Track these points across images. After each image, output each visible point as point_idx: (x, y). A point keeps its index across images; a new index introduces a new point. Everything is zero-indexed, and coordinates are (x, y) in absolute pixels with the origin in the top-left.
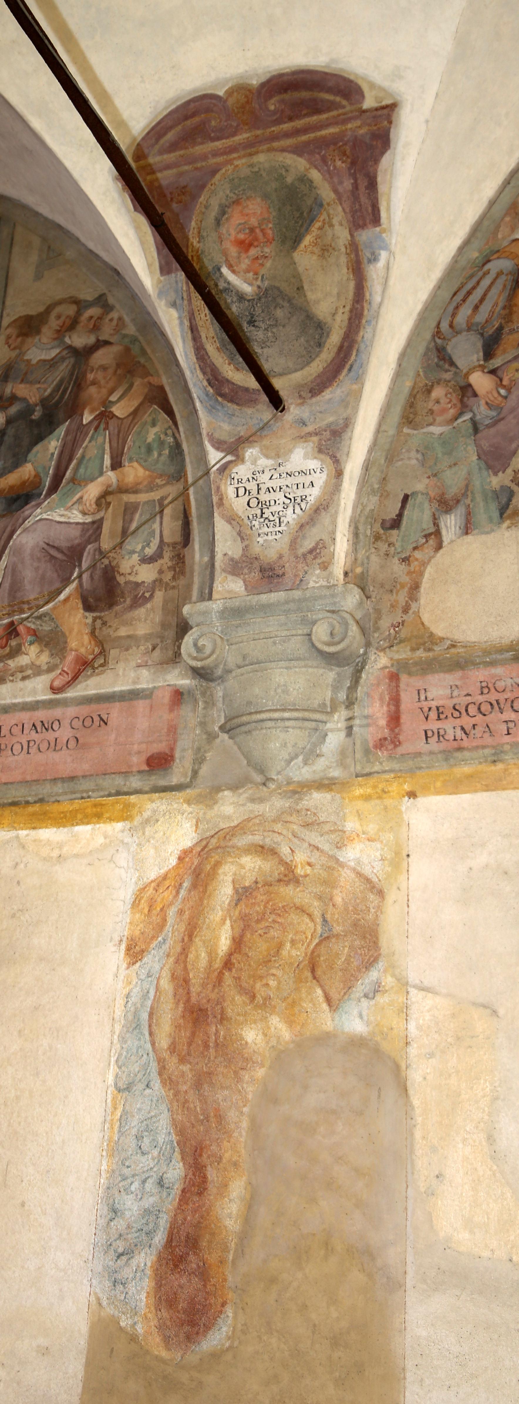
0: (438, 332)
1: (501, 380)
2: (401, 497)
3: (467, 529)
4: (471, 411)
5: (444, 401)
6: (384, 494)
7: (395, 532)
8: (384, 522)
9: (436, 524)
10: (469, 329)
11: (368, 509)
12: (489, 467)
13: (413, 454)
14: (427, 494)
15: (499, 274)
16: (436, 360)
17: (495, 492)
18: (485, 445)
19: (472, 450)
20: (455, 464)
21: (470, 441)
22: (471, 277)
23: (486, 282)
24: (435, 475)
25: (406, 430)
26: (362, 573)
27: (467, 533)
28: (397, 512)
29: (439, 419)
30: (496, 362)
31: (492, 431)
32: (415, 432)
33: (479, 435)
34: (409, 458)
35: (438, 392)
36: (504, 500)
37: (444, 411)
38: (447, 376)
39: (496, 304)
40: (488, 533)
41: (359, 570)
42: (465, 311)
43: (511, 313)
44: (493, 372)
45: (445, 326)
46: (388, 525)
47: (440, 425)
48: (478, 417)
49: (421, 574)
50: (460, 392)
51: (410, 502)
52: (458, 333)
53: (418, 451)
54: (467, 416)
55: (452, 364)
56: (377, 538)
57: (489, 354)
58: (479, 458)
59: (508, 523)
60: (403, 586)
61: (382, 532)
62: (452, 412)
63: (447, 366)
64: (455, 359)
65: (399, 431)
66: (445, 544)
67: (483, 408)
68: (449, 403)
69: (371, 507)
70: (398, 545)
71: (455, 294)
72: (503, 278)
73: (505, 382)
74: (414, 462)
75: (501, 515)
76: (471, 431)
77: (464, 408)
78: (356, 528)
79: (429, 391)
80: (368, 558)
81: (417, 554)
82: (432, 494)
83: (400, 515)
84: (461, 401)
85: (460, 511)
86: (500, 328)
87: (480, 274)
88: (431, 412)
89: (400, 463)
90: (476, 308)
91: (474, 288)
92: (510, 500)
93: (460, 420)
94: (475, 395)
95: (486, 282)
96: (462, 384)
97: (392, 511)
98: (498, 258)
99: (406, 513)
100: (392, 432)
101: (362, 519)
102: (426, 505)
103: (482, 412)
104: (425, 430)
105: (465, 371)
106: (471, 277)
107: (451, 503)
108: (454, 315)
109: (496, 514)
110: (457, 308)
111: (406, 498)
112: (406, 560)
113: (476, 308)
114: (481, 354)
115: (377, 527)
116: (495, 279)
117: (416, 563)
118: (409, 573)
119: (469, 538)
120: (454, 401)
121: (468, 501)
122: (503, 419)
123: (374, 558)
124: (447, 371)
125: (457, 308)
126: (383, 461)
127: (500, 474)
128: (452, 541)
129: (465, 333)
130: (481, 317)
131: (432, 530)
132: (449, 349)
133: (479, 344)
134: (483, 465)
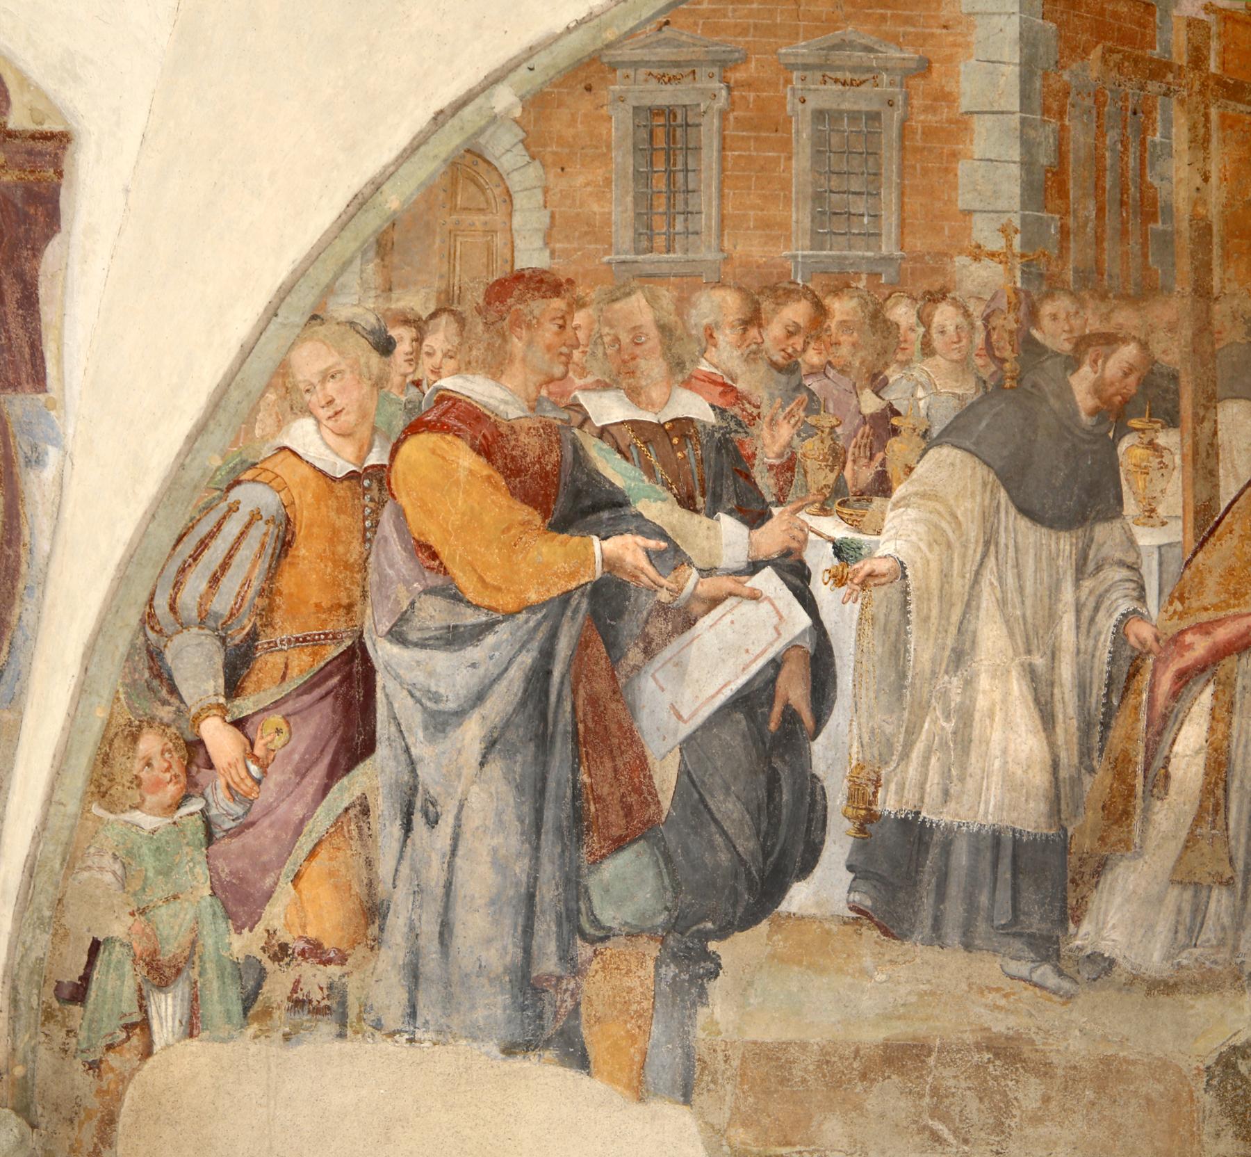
0: (151, 616)
1: (252, 744)
2: (88, 944)
3: (192, 1027)
4: (202, 795)
5: (158, 763)
6: (61, 934)
7: (76, 1009)
8: (59, 986)
9: (143, 1008)
10: (202, 624)
11: (33, 955)
12: (229, 915)
13: (107, 860)
14: (130, 947)
15: (255, 516)
16: (147, 675)
17: (236, 964)
18: (224, 868)
19: (202, 871)
20: (175, 897)
21: (200, 855)
22: (208, 508)
23: (232, 528)
24: (143, 912)
25: (96, 810)
26: (25, 1077)
27: (191, 1035)
28: (81, 972)
29: (151, 799)
30: (245, 706)
31: (236, 843)
32: (112, 817)
33: (214, 847)
34: (101, 869)
35: (150, 743)
36: (250, 984)
37: (158, 785)
38: (165, 713)
39: (247, 582)
40: (223, 1041)
41: (19, 1071)
42: (196, 583)
43: (271, 609)
44: (239, 724)
45: (162, 603)
46: (66, 993)
47: (151, 812)
48: (213, 812)
49: (119, 1098)
50: (184, 752)
51: (102, 956)
52: (184, 626)
53: (115, 857)
54: (195, 805)
55: (173, 690)
56: (49, 1016)
57: (233, 688)
58: (214, 894)
59: (253, 1028)
60: (89, 1117)
61: (56, 1005)
62: (172, 790)
63: (164, 692)
64: (178, 681)
65: (85, 811)
66: (156, 1048)
67: (222, 794)
68: (168, 769)
69: (37, 952)
70: (82, 1034)
71: (180, 540)
72: (259, 530)
73: (259, 751)
74: (108, 877)
75: (246, 1010)
76: (201, 836)
77: (191, 789)
78: (14, 988)
79: (135, 738)
80: (34, 1050)
81: (112, 1059)
82: (138, 949)
83: (86, 978)
84: (187, 771)
85: (181, 989)
86: (253, 636)
87: (223, 506)
88: (137, 781)
89: (86, 874)
90: (215, 580)
91: (212, 535)
92: (259, 986)
93: (184, 811)
94: (210, 766)
95: (232, 528)
96: (190, 737)
97: (73, 973)
98: (254, 480)
99: (95, 975)
100: (73, 807)
101: (24, 974)
102: (128, 966)
103: (223, 806)
104: (127, 817)
105: (194, 711)
106: (208, 508)
107: (167, 972)
108: (177, 585)
109: (237, 1008)
110: (183, 571)
111: (95, 947)
112: (94, 1066)
113: (215, 580)
114: (221, 681)
115: (49, 993)
116: (248, 526)
117: (111, 1075)
118: (100, 1092)
119: (194, 1045)
120: (176, 769)
121: (194, 974)
122: (252, 824)
123: (42, 1052)
124: (165, 703)
125: (183, 571)
126: (57, 866)
127: (245, 931)
128: (168, 1046)
129: (195, 630)
130: (222, 603)
131: (136, 1018)
132: (169, 655)
133: (219, 660)
134: (220, 911)
